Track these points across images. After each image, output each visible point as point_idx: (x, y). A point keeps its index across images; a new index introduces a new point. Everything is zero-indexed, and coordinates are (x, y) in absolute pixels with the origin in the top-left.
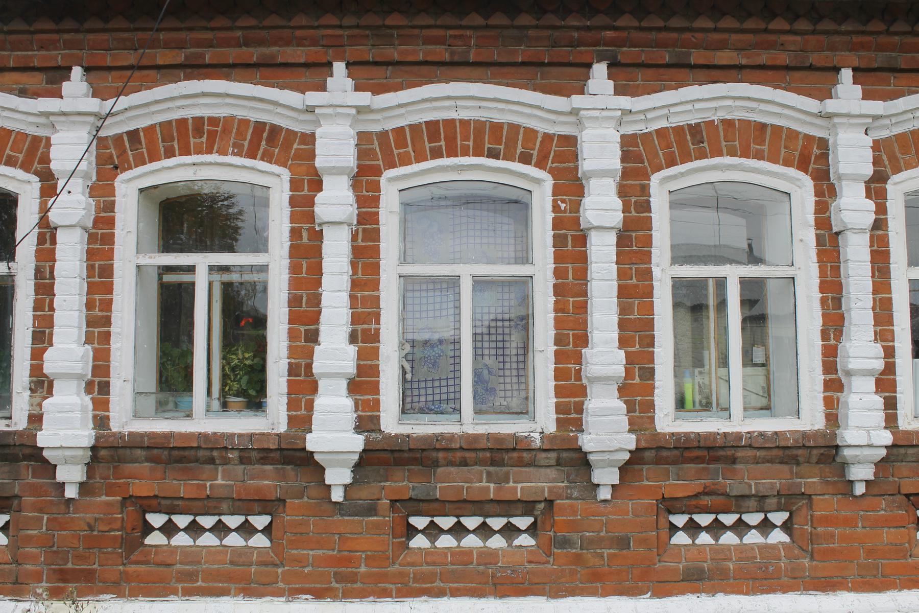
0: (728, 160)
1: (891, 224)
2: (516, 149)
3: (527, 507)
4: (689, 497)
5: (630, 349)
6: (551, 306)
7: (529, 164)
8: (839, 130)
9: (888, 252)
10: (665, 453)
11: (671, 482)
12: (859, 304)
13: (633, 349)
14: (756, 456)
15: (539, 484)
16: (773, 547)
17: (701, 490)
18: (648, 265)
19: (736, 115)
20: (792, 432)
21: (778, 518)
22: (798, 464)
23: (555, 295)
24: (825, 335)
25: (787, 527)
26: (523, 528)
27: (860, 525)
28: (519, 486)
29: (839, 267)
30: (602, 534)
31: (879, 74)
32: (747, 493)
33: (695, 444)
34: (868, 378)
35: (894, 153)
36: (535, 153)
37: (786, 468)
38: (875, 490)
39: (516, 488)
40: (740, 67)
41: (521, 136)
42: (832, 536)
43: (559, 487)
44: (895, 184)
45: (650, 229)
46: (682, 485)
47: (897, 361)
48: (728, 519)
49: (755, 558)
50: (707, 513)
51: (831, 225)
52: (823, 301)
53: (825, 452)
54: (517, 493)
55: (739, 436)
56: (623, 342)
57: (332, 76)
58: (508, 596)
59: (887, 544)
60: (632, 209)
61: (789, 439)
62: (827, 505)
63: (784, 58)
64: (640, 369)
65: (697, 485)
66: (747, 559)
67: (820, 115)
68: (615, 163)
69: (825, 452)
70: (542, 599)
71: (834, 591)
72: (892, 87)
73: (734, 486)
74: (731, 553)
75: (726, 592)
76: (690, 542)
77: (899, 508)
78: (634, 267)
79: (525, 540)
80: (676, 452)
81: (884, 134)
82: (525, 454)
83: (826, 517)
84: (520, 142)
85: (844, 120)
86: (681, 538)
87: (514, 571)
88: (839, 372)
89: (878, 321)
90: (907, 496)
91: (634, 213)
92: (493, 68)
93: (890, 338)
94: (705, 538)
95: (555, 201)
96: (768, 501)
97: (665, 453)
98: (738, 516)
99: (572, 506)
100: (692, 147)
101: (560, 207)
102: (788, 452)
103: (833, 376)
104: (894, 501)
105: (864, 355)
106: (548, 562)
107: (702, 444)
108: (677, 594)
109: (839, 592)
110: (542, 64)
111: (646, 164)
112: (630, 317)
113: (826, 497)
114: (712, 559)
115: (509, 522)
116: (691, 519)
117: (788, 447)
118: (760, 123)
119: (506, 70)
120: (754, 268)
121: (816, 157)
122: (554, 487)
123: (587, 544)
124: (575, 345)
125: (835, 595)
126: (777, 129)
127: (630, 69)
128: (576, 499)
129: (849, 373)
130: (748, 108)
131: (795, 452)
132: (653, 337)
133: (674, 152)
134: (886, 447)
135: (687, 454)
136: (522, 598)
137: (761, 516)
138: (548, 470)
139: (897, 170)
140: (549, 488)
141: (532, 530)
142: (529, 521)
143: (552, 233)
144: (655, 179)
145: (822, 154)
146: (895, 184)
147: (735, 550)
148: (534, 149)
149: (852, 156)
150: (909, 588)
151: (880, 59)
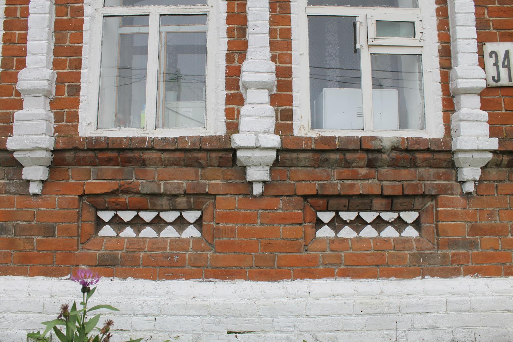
5: (61, 71)
11: (92, 181)
12: (257, 30)
14: (161, 158)
16: (186, 241)
17: (116, 188)
18: (81, 5)
21: (191, 216)
22: (203, 167)
23: (4, 29)
24: (229, 58)
25: (198, 223)
27: (259, 222)
30: (33, 223)
32: (156, 191)
33: (104, 146)
34: (262, 91)
37: (191, 170)
42: (233, 230)
46: (101, 183)
47: (294, 80)
48: (148, 216)
49: (165, 249)
52: (229, 32)
53: (223, 155)
55: (143, 140)
56: (56, 65)
59: (283, 239)
61: (187, 142)
62: (228, 204)
64: (68, 86)
65: (112, 185)
66: (158, 249)
69: (223, 155)
71: (233, 279)
74: (145, 244)
75: (136, 276)
76: (115, 234)
77: (295, 207)
80: (91, 154)
83: (227, 214)
86: (107, 231)
88: (241, 88)
89: (273, 46)
90: (305, 197)
93: (288, 60)
97: (82, 155)
98: (156, 213)
102: (190, 155)
103: (235, 92)
107: (110, 146)
109: (237, 280)
113: (229, 196)
114: (127, 249)
116: (116, 216)
120: (173, 7)
123: (20, 231)
125: (234, 283)
128: (14, 193)
132: (80, 61)
135: (100, 155)
137: (176, 214)
147: (150, 242)
150: (302, 278)
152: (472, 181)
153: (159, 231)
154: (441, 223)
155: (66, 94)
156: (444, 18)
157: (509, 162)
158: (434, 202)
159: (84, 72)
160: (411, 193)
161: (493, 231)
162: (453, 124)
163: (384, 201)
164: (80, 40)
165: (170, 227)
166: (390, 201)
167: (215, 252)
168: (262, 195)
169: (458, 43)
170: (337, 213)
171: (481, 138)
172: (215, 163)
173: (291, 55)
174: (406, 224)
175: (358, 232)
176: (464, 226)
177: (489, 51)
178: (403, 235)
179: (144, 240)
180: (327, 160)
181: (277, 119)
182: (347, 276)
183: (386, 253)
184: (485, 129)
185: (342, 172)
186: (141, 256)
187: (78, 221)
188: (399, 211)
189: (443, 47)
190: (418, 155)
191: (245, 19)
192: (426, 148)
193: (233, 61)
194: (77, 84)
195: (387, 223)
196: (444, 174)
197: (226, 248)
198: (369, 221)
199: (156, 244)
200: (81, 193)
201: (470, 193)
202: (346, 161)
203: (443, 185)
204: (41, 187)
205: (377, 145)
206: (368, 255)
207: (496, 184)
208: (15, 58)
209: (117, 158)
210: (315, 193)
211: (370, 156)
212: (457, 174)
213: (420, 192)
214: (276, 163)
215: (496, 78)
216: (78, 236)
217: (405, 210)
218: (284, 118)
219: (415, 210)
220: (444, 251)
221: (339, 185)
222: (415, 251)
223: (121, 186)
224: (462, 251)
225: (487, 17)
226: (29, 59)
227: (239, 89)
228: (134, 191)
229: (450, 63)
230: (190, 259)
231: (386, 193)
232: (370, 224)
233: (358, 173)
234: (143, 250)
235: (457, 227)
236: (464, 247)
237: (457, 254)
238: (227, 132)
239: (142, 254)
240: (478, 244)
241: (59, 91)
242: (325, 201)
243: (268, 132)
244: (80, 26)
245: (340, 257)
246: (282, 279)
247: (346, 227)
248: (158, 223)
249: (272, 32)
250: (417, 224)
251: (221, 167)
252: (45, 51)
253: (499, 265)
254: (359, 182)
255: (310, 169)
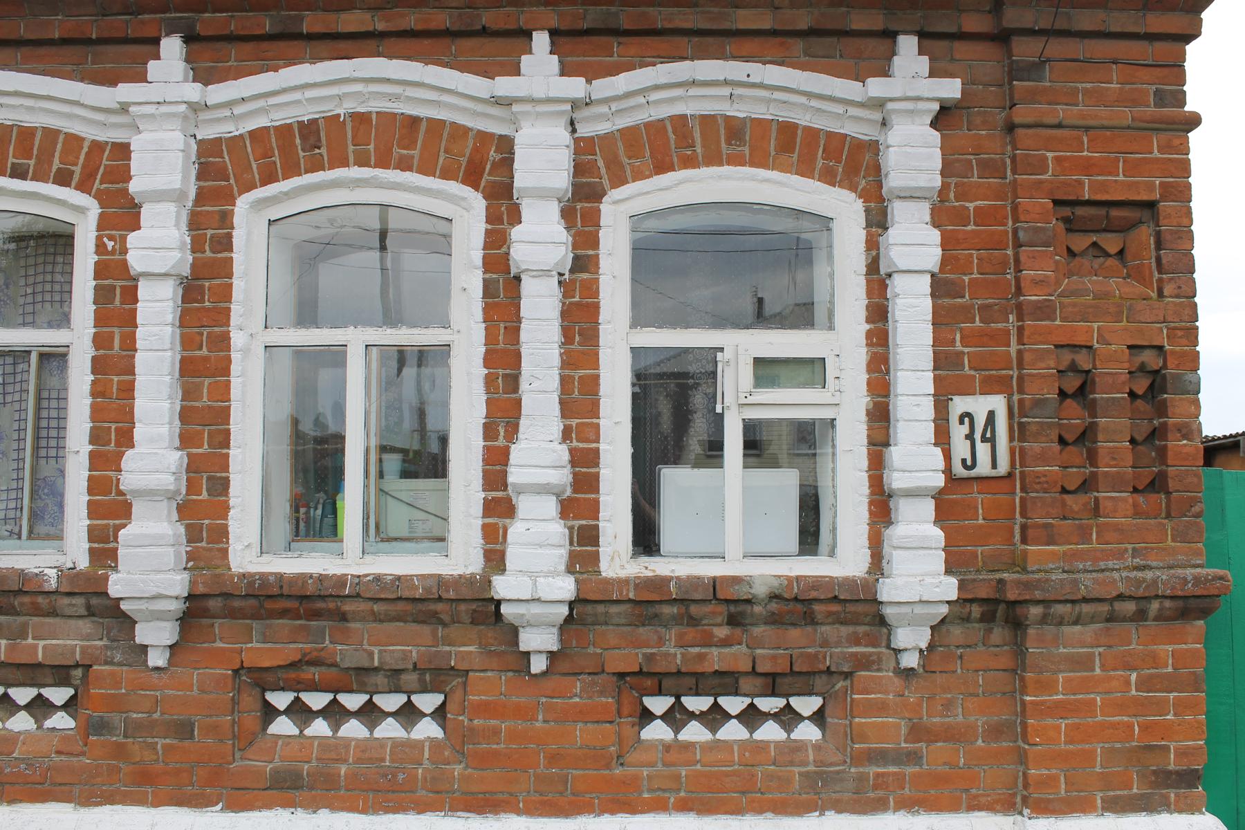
0: (355, 172)
1: (604, 263)
2: (50, 164)
3: (61, 674)
4: (279, 667)
6: (87, 388)
7: (67, 185)
8: (523, 124)
9: (596, 307)
10: (237, 603)
13: (200, 451)
14: (372, 610)
15: (69, 642)
16: (418, 745)
19: (374, 106)
20: (422, 577)
21: (427, 702)
22: (444, 625)
24: (489, 431)
25: (440, 714)
26: (59, 703)
27: (540, 717)
28: (42, 643)
29: (518, 329)
30: (156, 716)
31: (595, 39)
32: (366, 664)
33: (276, 591)
34: (544, 497)
35: (616, 156)
36: (77, 170)
37: (426, 629)
38: (564, 666)
39: (36, 646)
40: (383, 35)
41: (59, 146)
42: (496, 732)
43: (95, 647)
44: (616, 202)
45: (230, 276)
46: (270, 649)
48: (353, 701)
49: (383, 760)
50: (317, 690)
51: (509, 266)
52: (489, 382)
54: (36, 654)
55: (341, 580)
56: (186, 440)
57: (158, 58)
58: (21, 801)
60: (207, 248)
62: (490, 685)
63: (441, 19)
64: (209, 478)
65: (291, 651)
67: (498, 101)
68: (562, 180)
69: (478, 608)
70: (68, 807)
71: (496, 813)
72: (615, 58)
73: (347, 654)
74: (348, 752)
75: (333, 808)
76: (296, 732)
77: (602, 693)
78: (205, 331)
79: (61, 721)
80: (252, 602)
81: (603, 128)
82: (40, 599)
84: (57, 155)
85: (527, 107)
86: (283, 726)
87: (30, 766)
90: (622, 675)
91: (208, 254)
92: (25, 49)
94: (320, 727)
95: (99, 238)
96: (404, 677)
97: (237, 603)
98: (367, 697)
99: (112, 674)
100: (301, 154)
101: (105, 245)
102: (420, 606)
103: (500, 494)
104: (594, 683)
105: (534, 462)
106: (83, 754)
107: (286, 591)
108: (260, 808)
109: (503, 815)
110: (88, 42)
111: (232, 181)
112: (196, 404)
113: (489, 674)
115: (40, 695)
116: (297, 699)
117: (414, 600)
118: (410, 117)
119: (42, 51)
120: (389, 331)
121: (494, 165)
122: (88, 647)
123: (133, 729)
124: (118, 444)
125: (498, 820)
126: (436, 126)
127: (219, 45)
128: (120, 664)
129: (521, 489)
130: (389, 94)
131: (433, 607)
132: (228, 433)
133: (275, 162)
134: (948, 602)
135: (269, 605)
136: (38, 805)
137: (401, 699)
138: (80, 622)
139: (619, 180)
140: (82, 647)
141: (70, 706)
142: (67, 693)
143: (94, 283)
144: (243, 204)
145: (504, 159)
146: (616, 202)
147: (356, 746)
148: (76, 164)
149: (543, 163)
150: (613, 812)
151: (592, 16)
152: (914, 648)
153: (372, 727)
154: (857, 720)
155: (205, 492)
156: (880, 350)
157: (983, 614)
158: (848, 682)
159: (234, 453)
160: (805, 670)
161: (951, 735)
162: (886, 549)
163: (759, 681)
164: (224, 391)
165: (390, 720)
166: (770, 680)
167: (467, 767)
168: (544, 674)
169: (899, 403)
170: (678, 698)
171: (928, 580)
172: (466, 618)
173: (598, 425)
174: (801, 718)
175: (714, 730)
176: (898, 726)
177: (960, 413)
178: (793, 736)
179: (347, 741)
180: (656, 615)
181: (571, 543)
182: (690, 810)
183: (759, 771)
184: (938, 560)
185: (685, 633)
186: (342, 773)
187: (233, 712)
188: (787, 696)
189: (875, 404)
190: (817, 607)
191: (518, 356)
192: (830, 596)
193: (496, 439)
194: (224, 475)
195: (766, 716)
196: (867, 634)
197: (485, 760)
198: (734, 711)
199: (367, 748)
200: (237, 666)
201: (912, 669)
202: (691, 617)
203: (863, 654)
204: (168, 655)
205: (742, 592)
206: (727, 774)
207: (959, 651)
208: (113, 426)
209: (298, 609)
210: (637, 669)
211: (732, 609)
212: (890, 634)
213: (822, 667)
214: (569, 619)
215: (969, 463)
216: (234, 736)
217: (799, 695)
218: (586, 539)
219: (817, 694)
220: (861, 770)
221: (679, 656)
222: (811, 768)
223: (305, 655)
224: (892, 769)
225: (959, 346)
226: (139, 432)
227: (506, 489)
228: (329, 661)
229: (888, 435)
230: (425, 779)
231: (759, 669)
232: (736, 717)
233: (711, 635)
234: (345, 761)
235: (888, 728)
236: (896, 762)
237: (883, 774)
238: (485, 567)
239: (343, 769)
240: (921, 757)
241: (192, 487)
242: (656, 680)
243: (552, 574)
244: (224, 369)
245: (679, 777)
246: (579, 814)
247: (694, 722)
248: (370, 713)
249: (565, 382)
250: (819, 717)
251: (477, 624)
252: (167, 420)
253: (958, 793)
254: (715, 651)
255: (629, 628)
